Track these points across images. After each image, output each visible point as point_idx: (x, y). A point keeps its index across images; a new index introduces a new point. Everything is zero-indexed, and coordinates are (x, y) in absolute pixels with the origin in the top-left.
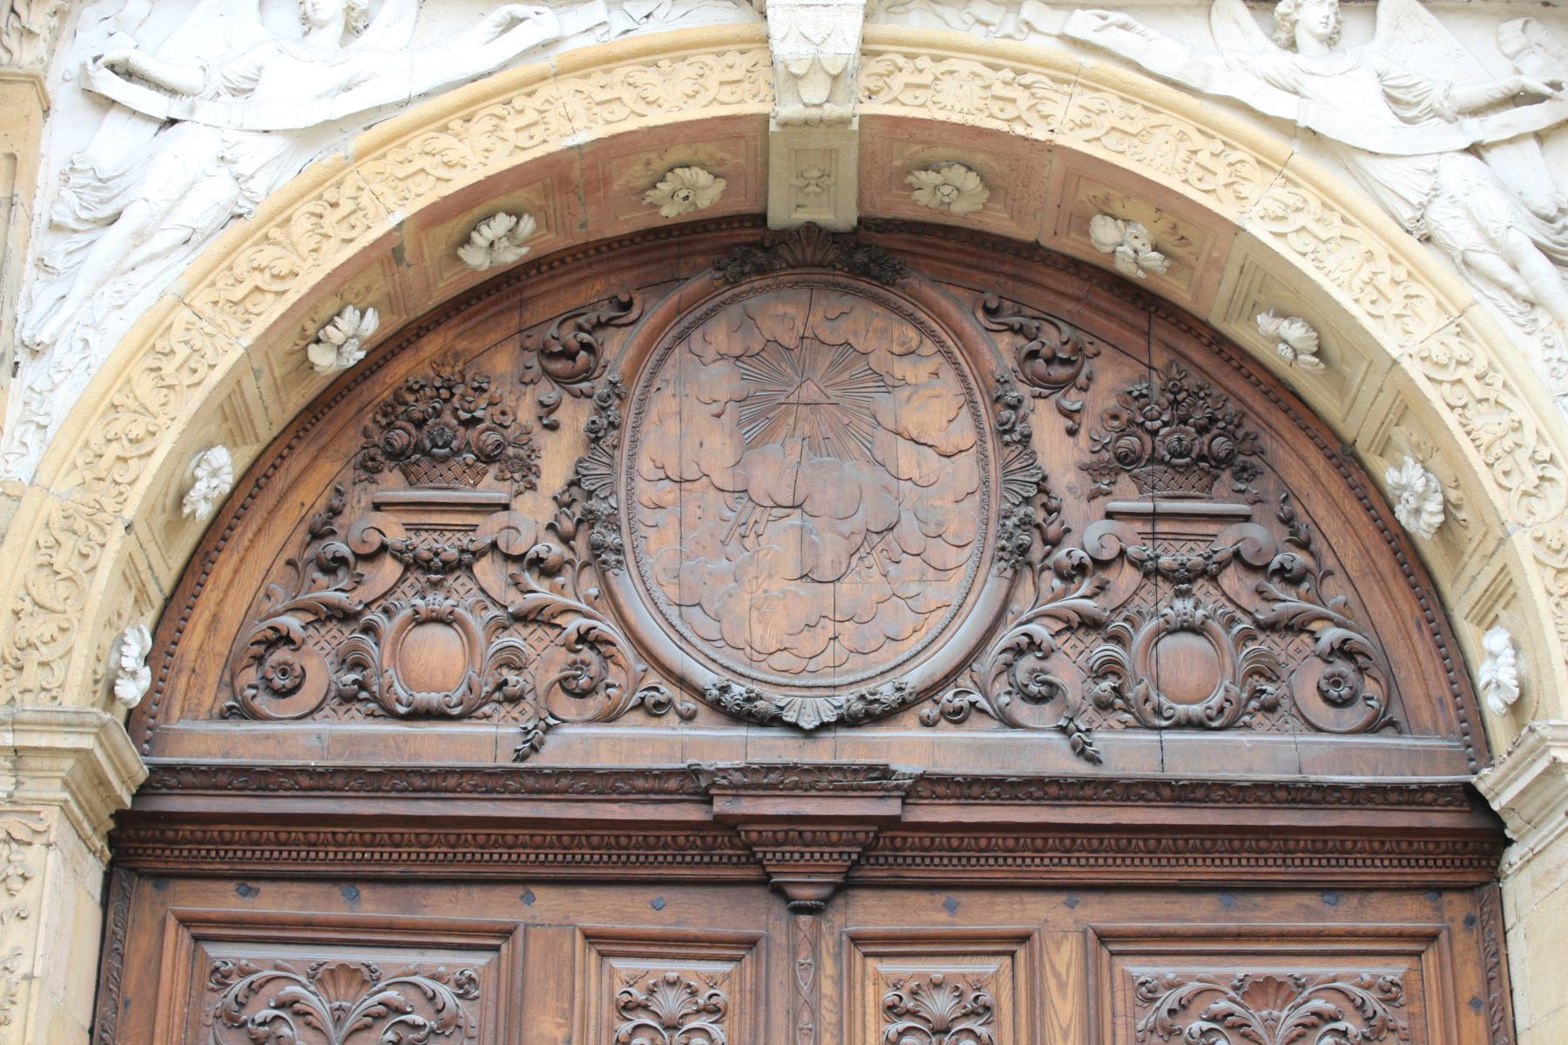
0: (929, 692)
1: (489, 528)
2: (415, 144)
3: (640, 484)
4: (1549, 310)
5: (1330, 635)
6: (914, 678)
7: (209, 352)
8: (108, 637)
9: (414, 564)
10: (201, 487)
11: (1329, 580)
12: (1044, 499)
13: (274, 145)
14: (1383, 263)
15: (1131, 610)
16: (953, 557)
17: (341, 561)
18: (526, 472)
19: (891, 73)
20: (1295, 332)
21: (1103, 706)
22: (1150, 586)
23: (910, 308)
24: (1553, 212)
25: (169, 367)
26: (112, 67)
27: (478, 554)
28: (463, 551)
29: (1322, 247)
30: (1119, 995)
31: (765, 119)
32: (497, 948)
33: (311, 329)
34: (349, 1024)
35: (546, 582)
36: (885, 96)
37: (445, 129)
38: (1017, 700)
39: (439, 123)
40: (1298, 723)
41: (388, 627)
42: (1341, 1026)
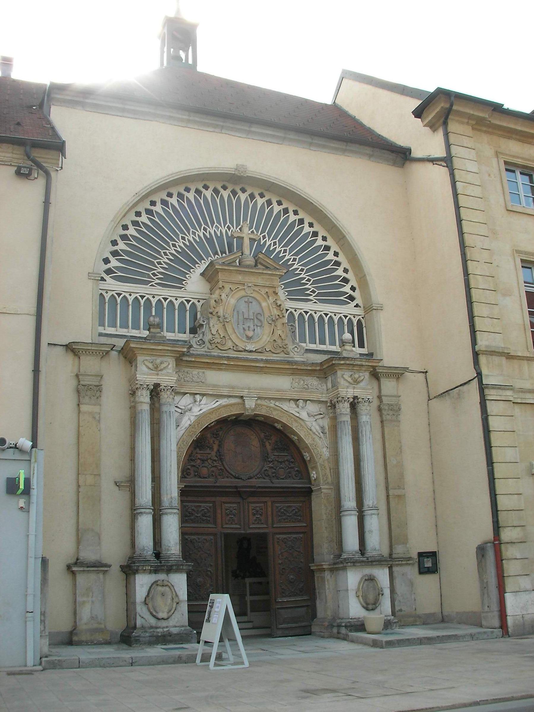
0: (256, 475)
5: (297, 469)
6: (255, 474)
18: (211, 448)
41: (200, 468)
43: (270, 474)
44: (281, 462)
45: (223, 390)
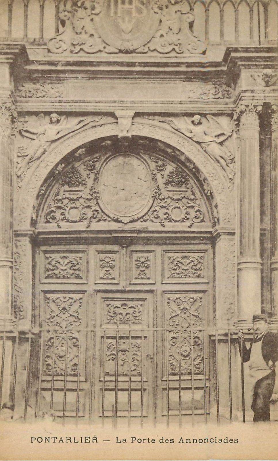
0: (142, 217)
1: (80, 194)
5: (197, 208)
9: (70, 200)
15: (170, 205)
17: (60, 200)
41: (67, 209)
44: (178, 200)
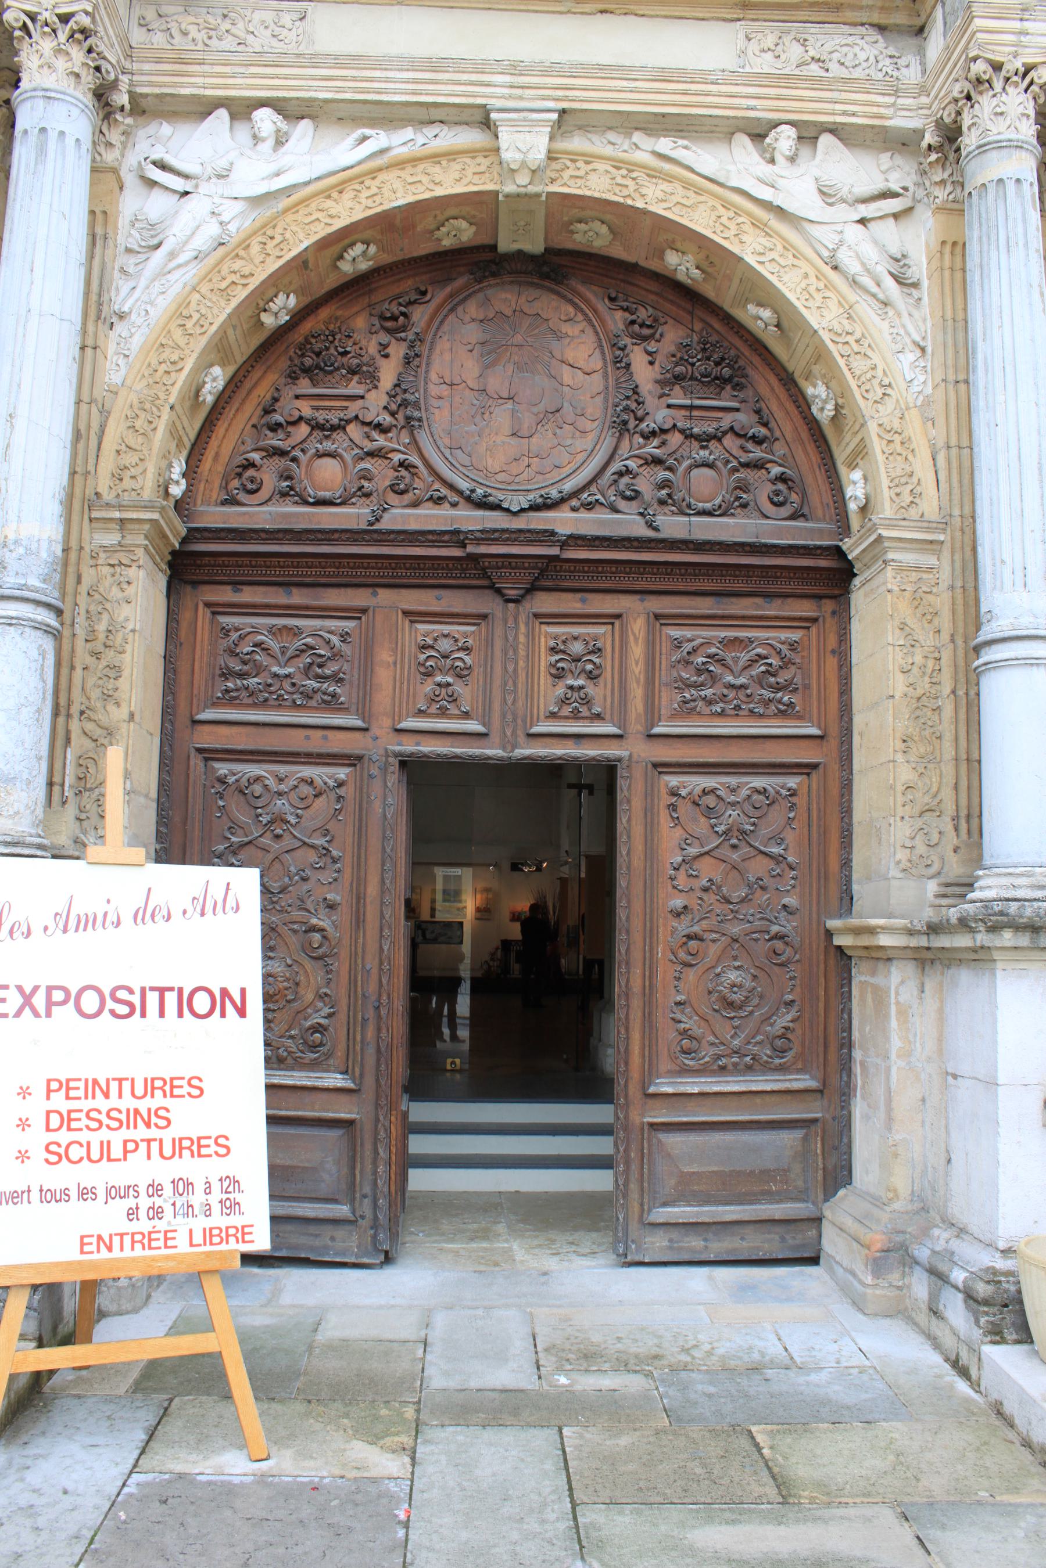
0: (575, 494)
1: (354, 407)
2: (314, 206)
3: (431, 386)
4: (894, 307)
5: (776, 470)
6: (568, 486)
7: (210, 316)
8: (164, 464)
9: (317, 426)
10: (208, 386)
11: (777, 443)
12: (636, 397)
13: (239, 206)
14: (812, 280)
15: (678, 455)
16: (589, 426)
17: (279, 425)
18: (372, 379)
19: (563, 170)
20: (766, 314)
21: (662, 502)
22: (688, 443)
23: (570, 296)
24: (899, 257)
25: (189, 324)
26: (154, 163)
27: (349, 422)
28: (341, 420)
29: (782, 270)
30: (664, 644)
31: (497, 193)
32: (360, 618)
33: (261, 304)
34: (289, 654)
35: (383, 436)
36: (559, 182)
37: (329, 197)
38: (619, 498)
39: (326, 193)
40: (757, 514)
41: (303, 458)
42: (769, 661)
43: (644, 485)
45: (387, 80)
